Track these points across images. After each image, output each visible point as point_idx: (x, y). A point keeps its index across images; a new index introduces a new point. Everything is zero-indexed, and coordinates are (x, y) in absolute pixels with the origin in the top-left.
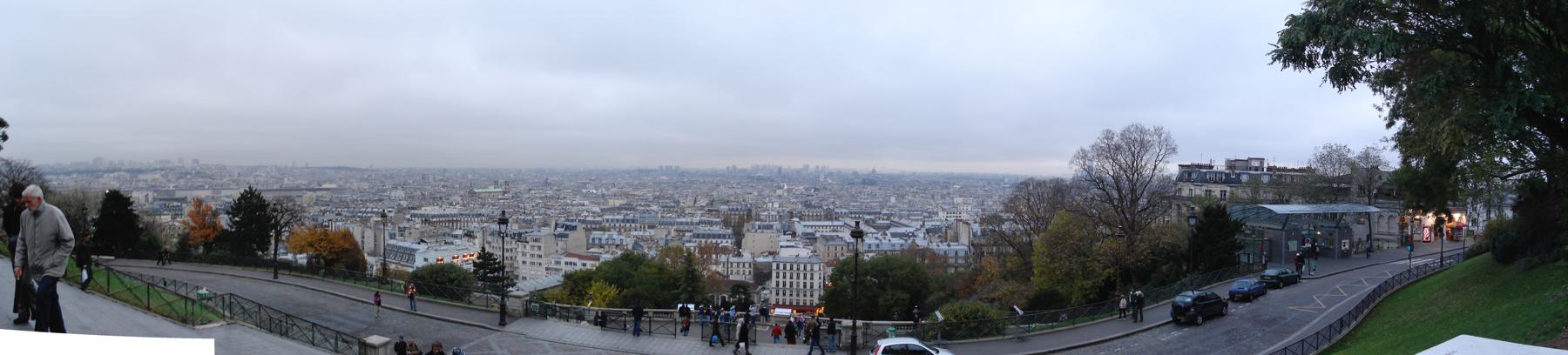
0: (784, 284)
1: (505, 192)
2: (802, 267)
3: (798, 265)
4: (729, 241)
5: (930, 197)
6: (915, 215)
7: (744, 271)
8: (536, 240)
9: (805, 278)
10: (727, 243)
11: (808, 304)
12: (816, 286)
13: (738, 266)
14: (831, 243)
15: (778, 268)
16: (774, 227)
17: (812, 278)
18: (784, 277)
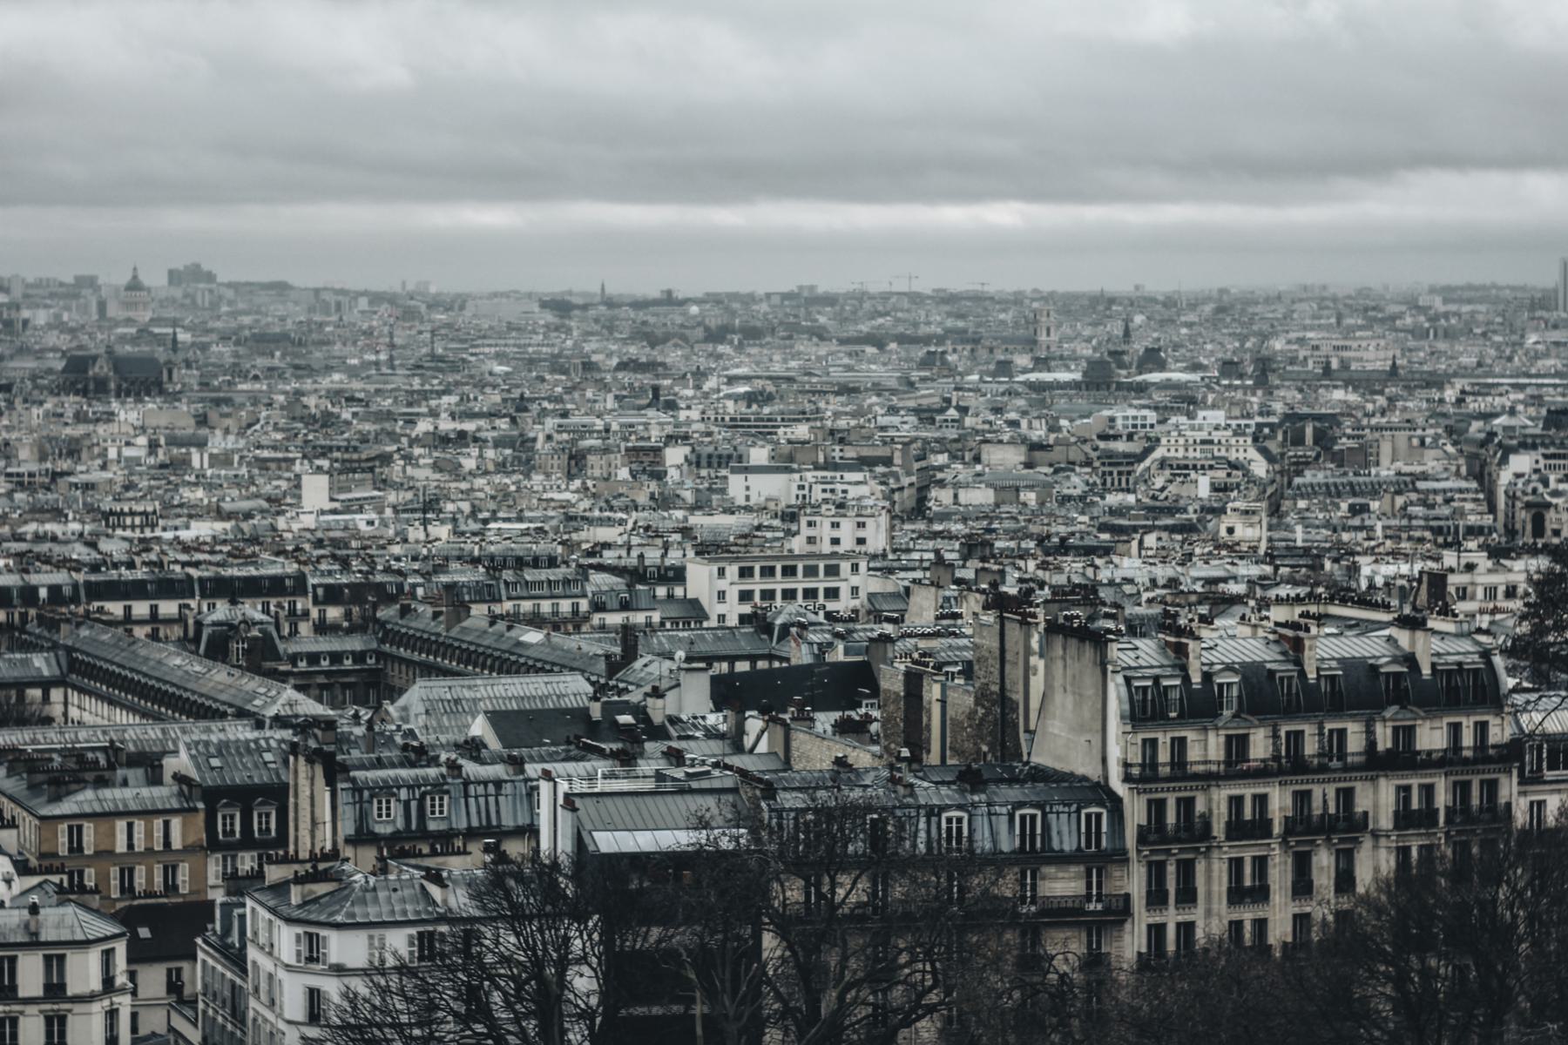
5: (558, 463)
6: (530, 590)
14: (85, 799)
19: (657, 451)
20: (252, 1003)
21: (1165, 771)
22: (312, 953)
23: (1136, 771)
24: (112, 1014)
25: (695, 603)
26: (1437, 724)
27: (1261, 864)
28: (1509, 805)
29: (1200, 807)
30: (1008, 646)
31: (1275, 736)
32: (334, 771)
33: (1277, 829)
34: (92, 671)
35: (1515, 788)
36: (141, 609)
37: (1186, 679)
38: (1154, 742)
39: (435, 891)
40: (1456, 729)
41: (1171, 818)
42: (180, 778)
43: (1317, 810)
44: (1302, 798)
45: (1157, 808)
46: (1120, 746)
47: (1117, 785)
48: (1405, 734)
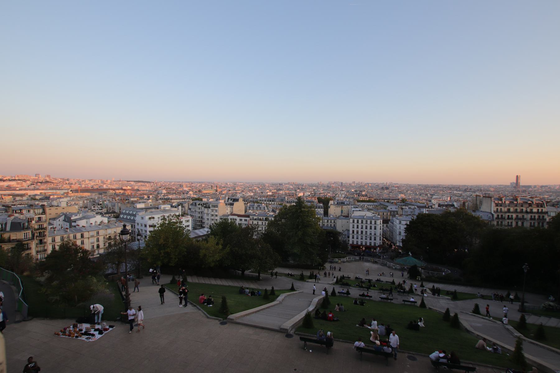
0: (357, 232)
1: (217, 191)
2: (369, 222)
3: (366, 221)
4: (322, 210)
7: (331, 225)
8: (214, 206)
9: (371, 228)
10: (321, 211)
11: (373, 244)
12: (378, 234)
13: (328, 222)
15: (354, 222)
16: (346, 203)
17: (375, 229)
18: (358, 227)
19: (427, 194)
20: (394, 227)
21: (499, 212)
22: (400, 223)
23: (495, 212)
24: (381, 227)
25: (432, 203)
26: (536, 209)
27: (511, 223)
28: (546, 219)
29: (504, 216)
30: (477, 199)
31: (514, 209)
32: (402, 209)
33: (514, 219)
34: (382, 204)
35: (547, 217)
36: (386, 201)
37: (502, 202)
38: (497, 209)
39: (413, 218)
40: (538, 210)
41: (500, 216)
42: (388, 209)
43: (519, 217)
44: (517, 216)
45: (498, 216)
46: (494, 208)
47: (493, 213)
48: (532, 210)
